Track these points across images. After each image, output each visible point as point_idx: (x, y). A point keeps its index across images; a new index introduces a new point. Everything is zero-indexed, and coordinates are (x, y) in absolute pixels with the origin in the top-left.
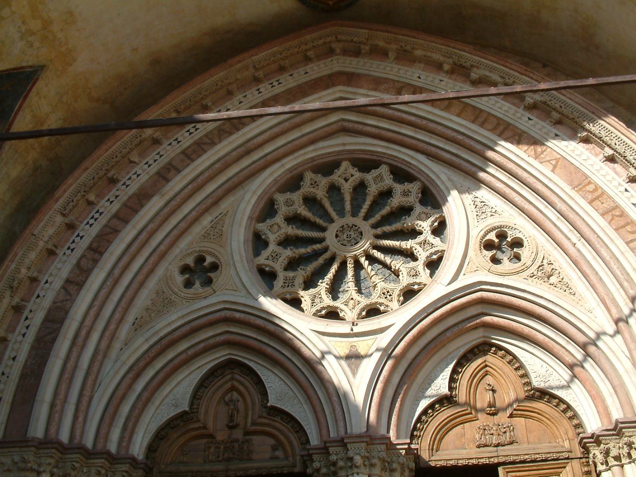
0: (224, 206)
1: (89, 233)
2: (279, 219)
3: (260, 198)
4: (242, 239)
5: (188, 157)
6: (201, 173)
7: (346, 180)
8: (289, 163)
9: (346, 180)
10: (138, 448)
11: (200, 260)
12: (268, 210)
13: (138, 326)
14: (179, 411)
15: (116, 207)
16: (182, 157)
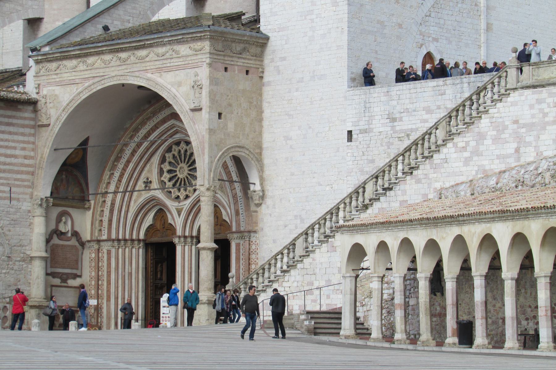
0: (152, 160)
1: (117, 174)
2: (167, 164)
3: (161, 157)
4: (156, 173)
5: (138, 147)
6: (142, 153)
7: (182, 149)
8: (167, 144)
9: (182, 149)
10: (142, 236)
11: (148, 179)
12: (163, 160)
13: (135, 202)
14: (150, 224)
15: (122, 166)
16: (137, 147)
